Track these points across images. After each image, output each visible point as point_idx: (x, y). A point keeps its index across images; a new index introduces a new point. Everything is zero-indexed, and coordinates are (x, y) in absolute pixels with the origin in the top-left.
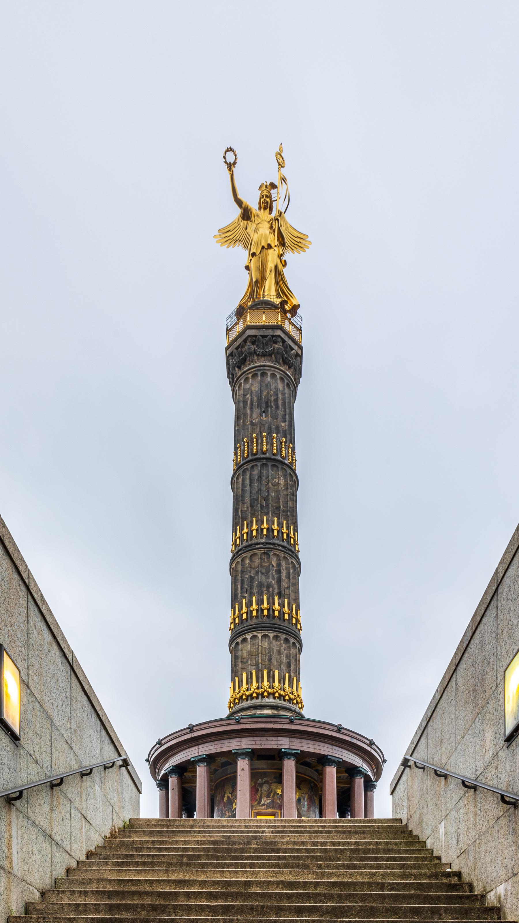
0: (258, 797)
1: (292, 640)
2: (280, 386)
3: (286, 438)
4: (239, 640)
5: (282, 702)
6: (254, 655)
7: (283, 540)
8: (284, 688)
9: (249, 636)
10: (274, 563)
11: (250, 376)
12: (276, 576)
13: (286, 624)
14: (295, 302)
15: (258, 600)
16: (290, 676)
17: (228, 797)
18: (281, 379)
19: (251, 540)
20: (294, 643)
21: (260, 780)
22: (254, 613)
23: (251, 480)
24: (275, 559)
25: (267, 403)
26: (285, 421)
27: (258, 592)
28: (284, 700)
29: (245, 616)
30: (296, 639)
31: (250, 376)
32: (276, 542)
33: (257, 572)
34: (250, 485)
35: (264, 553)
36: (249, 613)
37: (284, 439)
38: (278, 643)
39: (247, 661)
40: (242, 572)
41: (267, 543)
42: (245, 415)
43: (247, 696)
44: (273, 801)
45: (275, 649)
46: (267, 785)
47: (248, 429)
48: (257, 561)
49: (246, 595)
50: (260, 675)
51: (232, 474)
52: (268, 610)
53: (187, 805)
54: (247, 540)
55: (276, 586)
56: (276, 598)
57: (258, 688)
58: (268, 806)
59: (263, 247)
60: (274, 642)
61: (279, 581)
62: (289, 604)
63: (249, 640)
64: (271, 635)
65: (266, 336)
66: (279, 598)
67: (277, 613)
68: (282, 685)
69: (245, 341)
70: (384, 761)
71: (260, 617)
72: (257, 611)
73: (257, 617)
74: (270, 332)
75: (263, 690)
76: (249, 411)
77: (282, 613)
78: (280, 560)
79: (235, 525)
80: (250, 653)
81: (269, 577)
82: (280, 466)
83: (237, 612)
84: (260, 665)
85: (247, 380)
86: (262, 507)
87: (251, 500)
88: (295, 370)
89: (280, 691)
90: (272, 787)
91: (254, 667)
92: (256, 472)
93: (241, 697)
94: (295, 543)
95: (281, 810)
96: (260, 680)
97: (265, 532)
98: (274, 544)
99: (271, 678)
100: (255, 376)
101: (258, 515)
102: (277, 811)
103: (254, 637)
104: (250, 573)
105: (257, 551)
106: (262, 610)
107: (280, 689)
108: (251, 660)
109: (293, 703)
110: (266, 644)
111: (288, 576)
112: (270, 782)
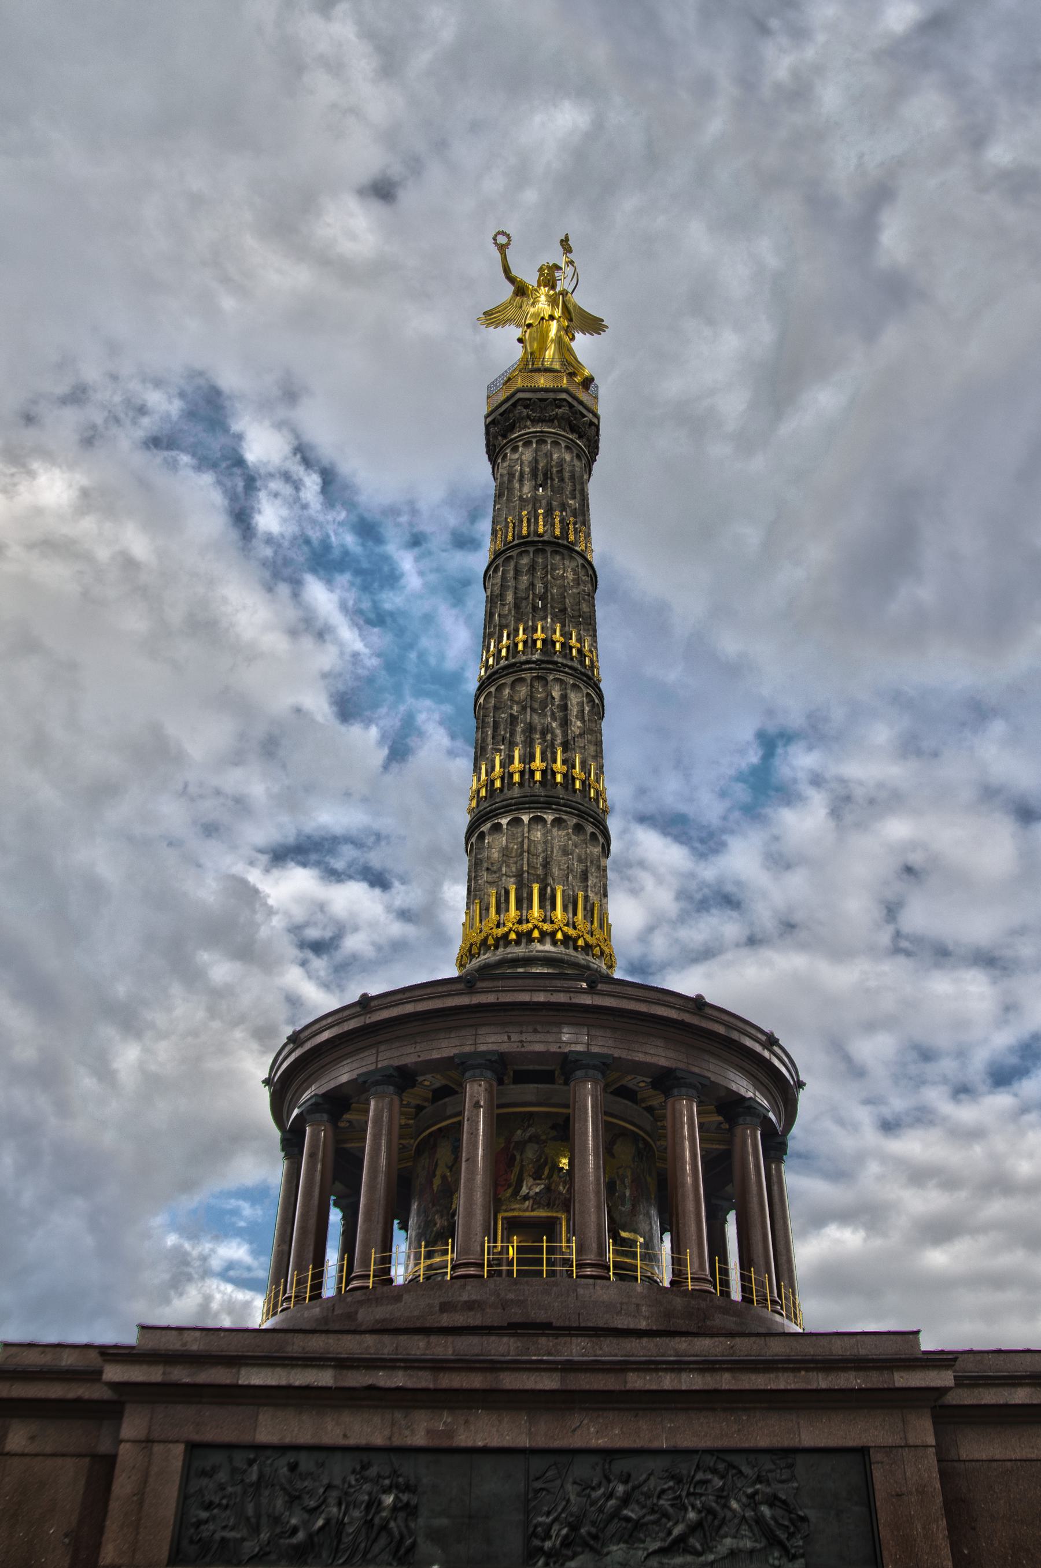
0: (513, 1177)
1: (590, 829)
2: (568, 457)
3: (575, 517)
4: (486, 827)
5: (571, 951)
6: (513, 855)
7: (572, 659)
8: (574, 923)
10: (556, 694)
11: (520, 444)
13: (578, 797)
14: (586, 373)
15: (525, 755)
16: (586, 898)
17: (444, 1177)
18: (567, 447)
19: (513, 657)
20: (593, 834)
21: (519, 1132)
22: (517, 778)
23: (517, 572)
24: (557, 688)
25: (545, 475)
26: (574, 498)
27: (524, 742)
28: (576, 948)
29: (498, 784)
30: (598, 828)
31: (520, 444)
32: (560, 660)
33: (524, 708)
34: (515, 578)
35: (538, 678)
36: (507, 777)
37: (572, 519)
38: (562, 833)
39: (500, 869)
40: (496, 708)
41: (543, 662)
42: (510, 490)
43: (497, 940)
44: (548, 1189)
45: (557, 844)
46: (536, 1147)
47: (515, 507)
50: (525, 895)
51: (486, 565)
54: (507, 658)
55: (558, 732)
57: (520, 922)
58: (537, 1201)
60: (555, 831)
61: (565, 723)
62: (583, 764)
63: (505, 827)
65: (545, 400)
66: (564, 752)
67: (559, 778)
68: (571, 915)
69: (514, 405)
70: (800, 1085)
71: (527, 784)
72: (522, 773)
73: (521, 784)
74: (551, 395)
75: (530, 925)
76: (517, 485)
78: (566, 689)
79: (487, 637)
80: (505, 852)
81: (546, 715)
82: (565, 552)
83: (483, 776)
84: (526, 875)
85: (515, 449)
87: (516, 598)
88: (589, 440)
89: (565, 929)
91: (512, 880)
92: (525, 561)
93: (486, 939)
94: (593, 666)
95: (568, 1212)
96: (525, 906)
97: (539, 644)
98: (556, 663)
99: (548, 901)
100: (527, 444)
101: (527, 621)
102: (559, 1215)
103: (516, 822)
104: (511, 708)
106: (532, 773)
107: (567, 925)
108: (508, 866)
109: (593, 955)
110: (538, 835)
111: (581, 715)
112: (543, 1137)
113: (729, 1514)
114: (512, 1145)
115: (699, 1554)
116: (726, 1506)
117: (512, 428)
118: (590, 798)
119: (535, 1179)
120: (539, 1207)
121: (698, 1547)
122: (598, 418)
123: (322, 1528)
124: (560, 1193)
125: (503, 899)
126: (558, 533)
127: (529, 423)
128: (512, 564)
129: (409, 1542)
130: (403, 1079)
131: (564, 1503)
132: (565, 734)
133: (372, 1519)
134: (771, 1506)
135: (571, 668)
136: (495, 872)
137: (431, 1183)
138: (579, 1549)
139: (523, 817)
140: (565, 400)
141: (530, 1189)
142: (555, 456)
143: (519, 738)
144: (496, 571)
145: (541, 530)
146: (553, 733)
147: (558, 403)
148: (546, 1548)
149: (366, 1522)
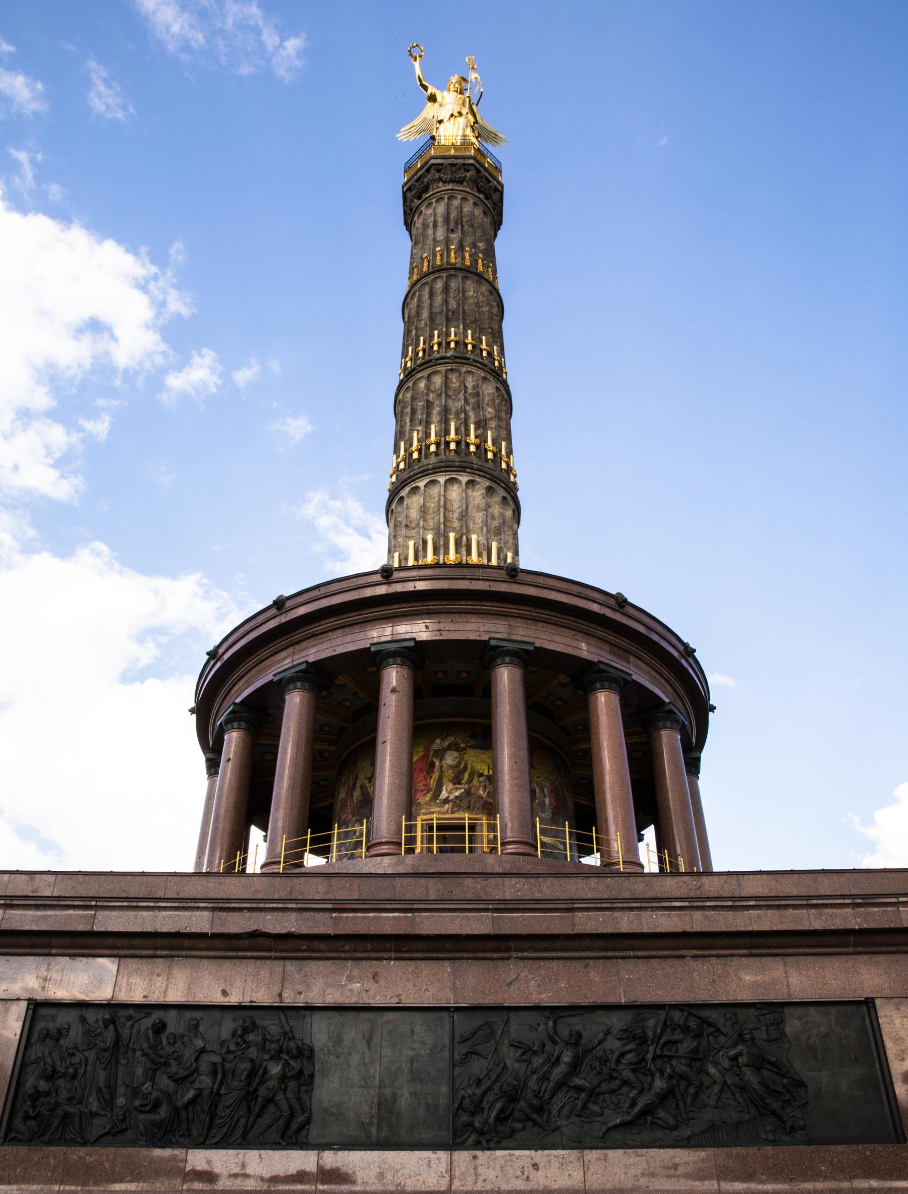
0: (433, 782)
1: (502, 493)
4: (404, 492)
9: (421, 484)
11: (434, 200)
12: (472, 401)
17: (362, 787)
21: (438, 741)
22: (433, 448)
23: (432, 294)
25: (456, 223)
29: (415, 455)
30: (509, 493)
31: (434, 200)
35: (452, 370)
36: (423, 450)
41: (456, 357)
44: (468, 792)
46: (455, 754)
48: (438, 380)
49: (420, 428)
50: (442, 543)
52: (458, 443)
53: (250, 804)
56: (472, 426)
58: (457, 804)
59: (452, 115)
61: (478, 407)
63: (422, 488)
64: (464, 478)
67: (472, 448)
72: (438, 444)
73: (437, 454)
77: (481, 448)
80: (424, 510)
86: (448, 320)
90: (467, 757)
92: (439, 285)
96: (442, 551)
98: (468, 359)
100: (440, 200)
105: (438, 368)
108: (425, 520)
110: (455, 493)
112: (463, 745)
113: (706, 1080)
114: (432, 753)
115: (675, 1128)
116: (702, 1071)
117: (426, 189)
118: (502, 469)
119: (454, 784)
120: (458, 810)
121: (671, 1121)
122: (502, 186)
123: (192, 1101)
124: (480, 797)
125: (421, 548)
126: (468, 263)
127: (441, 184)
128: (427, 289)
129: (301, 1119)
130: (317, 676)
131: (500, 1069)
132: (477, 415)
133: (256, 1090)
134: (759, 1069)
135: (481, 364)
136: (413, 529)
137: (352, 796)
138: (518, 1125)
139: (439, 479)
140: (472, 165)
141: (450, 793)
142: (465, 210)
143: (435, 418)
144: (412, 298)
145: (453, 261)
146: (466, 414)
147: (466, 167)
148: (477, 1124)
149: (248, 1093)
